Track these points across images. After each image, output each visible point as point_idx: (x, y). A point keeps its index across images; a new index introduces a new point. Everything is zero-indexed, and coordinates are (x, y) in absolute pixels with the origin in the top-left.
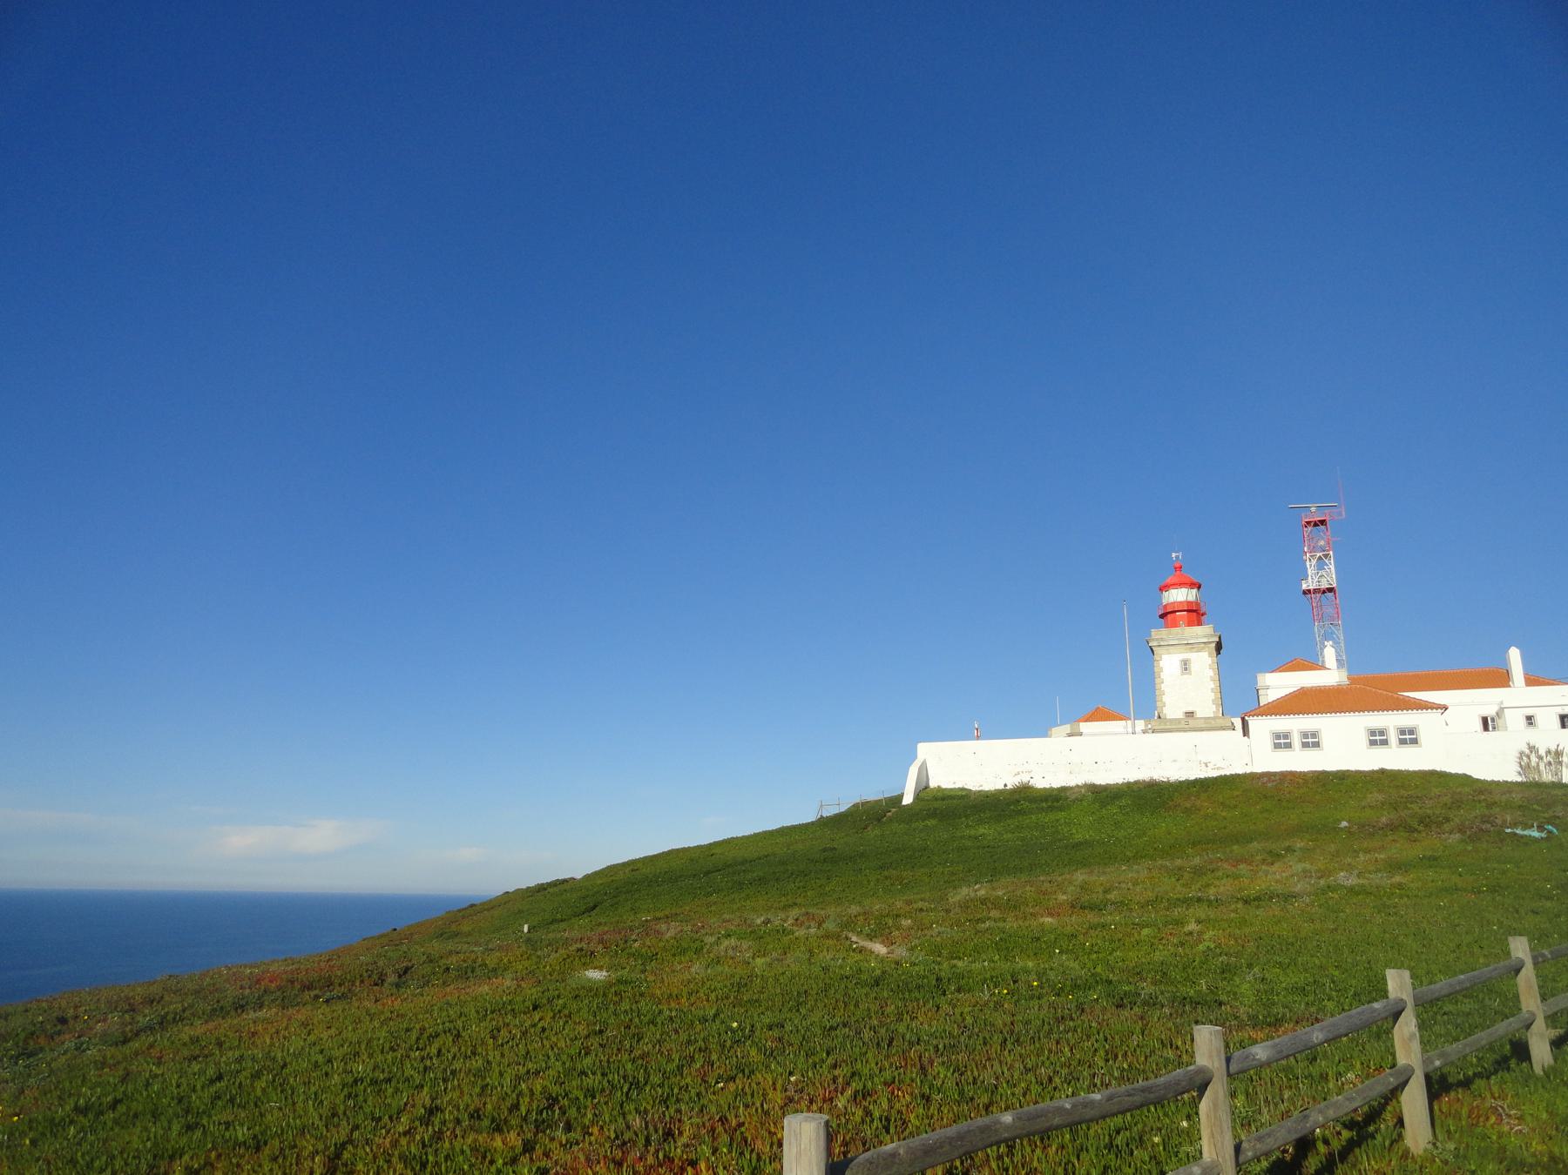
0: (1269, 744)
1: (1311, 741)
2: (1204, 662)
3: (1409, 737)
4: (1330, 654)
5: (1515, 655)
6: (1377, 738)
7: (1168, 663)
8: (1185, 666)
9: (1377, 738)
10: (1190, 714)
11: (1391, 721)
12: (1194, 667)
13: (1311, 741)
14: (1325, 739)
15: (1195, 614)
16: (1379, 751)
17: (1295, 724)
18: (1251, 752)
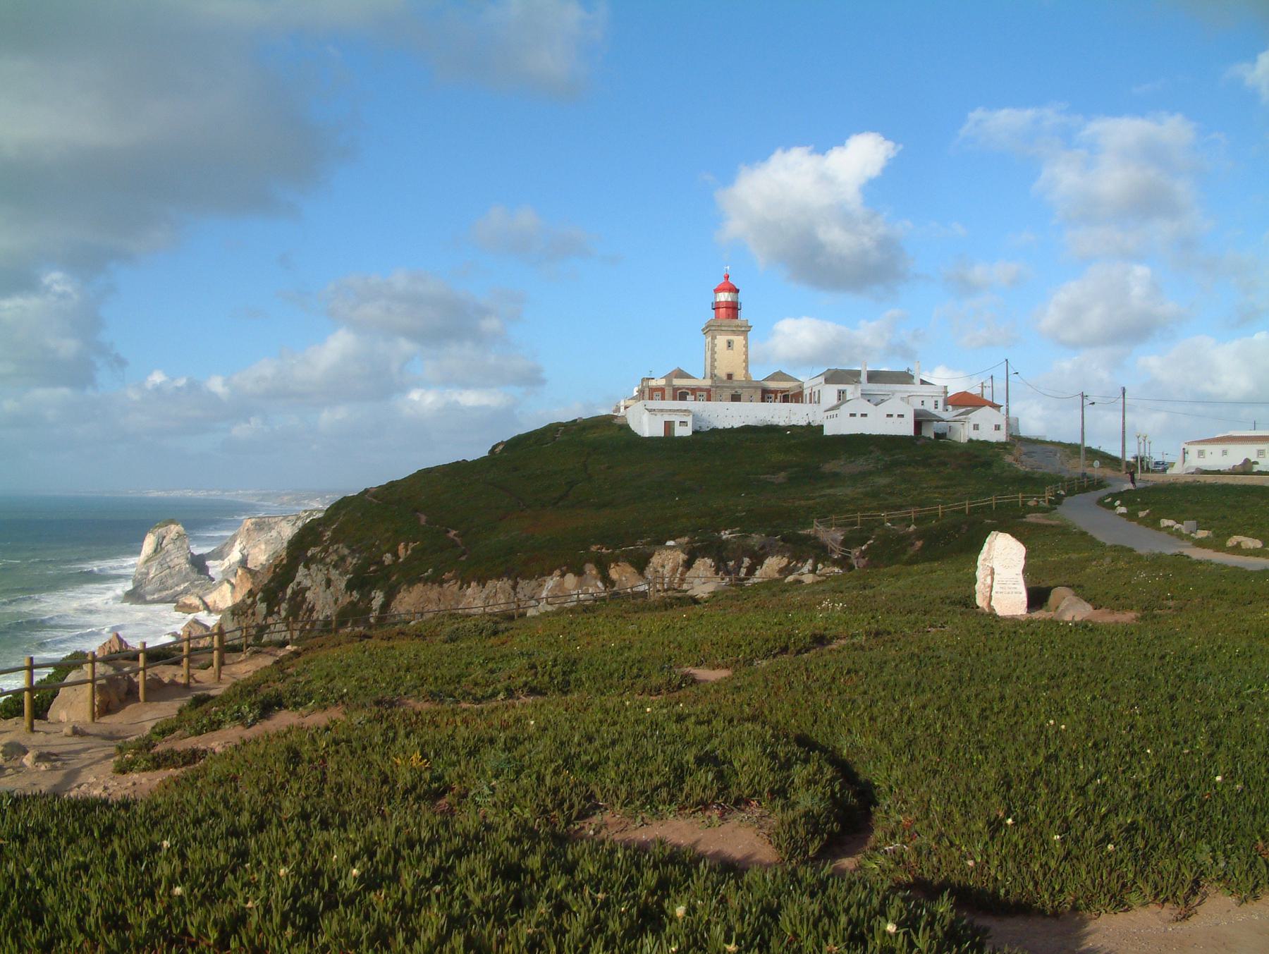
8: (729, 344)
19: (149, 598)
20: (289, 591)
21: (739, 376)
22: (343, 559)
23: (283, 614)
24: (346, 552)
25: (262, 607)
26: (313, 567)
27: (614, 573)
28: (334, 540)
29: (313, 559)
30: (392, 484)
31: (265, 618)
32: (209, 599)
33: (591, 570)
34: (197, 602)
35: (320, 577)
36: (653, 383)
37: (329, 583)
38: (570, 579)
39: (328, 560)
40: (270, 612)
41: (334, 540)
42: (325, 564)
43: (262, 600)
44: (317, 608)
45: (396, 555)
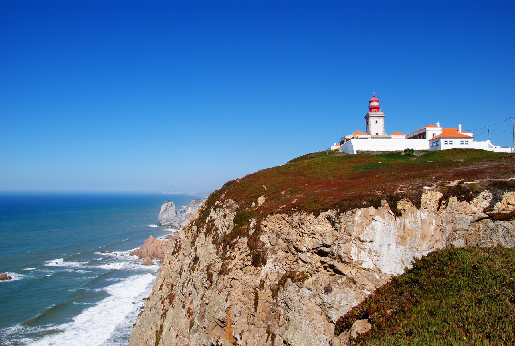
0: (444, 142)
1: (451, 143)
2: (381, 121)
3: (467, 143)
4: (438, 124)
5: (460, 125)
6: (462, 143)
7: (372, 121)
9: (462, 143)
10: (377, 134)
11: (464, 140)
12: (378, 122)
13: (451, 143)
14: (453, 143)
15: (377, 108)
16: (462, 145)
17: (448, 140)
18: (398, 144)
19: (163, 224)
20: (207, 221)
21: (381, 133)
22: (232, 205)
23: (205, 230)
24: (233, 202)
25: (195, 228)
26: (218, 209)
27: (399, 207)
28: (225, 198)
29: (218, 206)
30: (248, 176)
31: (197, 232)
32: (181, 225)
33: (384, 203)
34: (176, 225)
35: (221, 214)
36: (347, 137)
37: (225, 216)
38: (372, 210)
39: (224, 206)
40: (198, 230)
41: (225, 198)
42: (223, 208)
43: (196, 225)
44: (220, 228)
45: (256, 203)
